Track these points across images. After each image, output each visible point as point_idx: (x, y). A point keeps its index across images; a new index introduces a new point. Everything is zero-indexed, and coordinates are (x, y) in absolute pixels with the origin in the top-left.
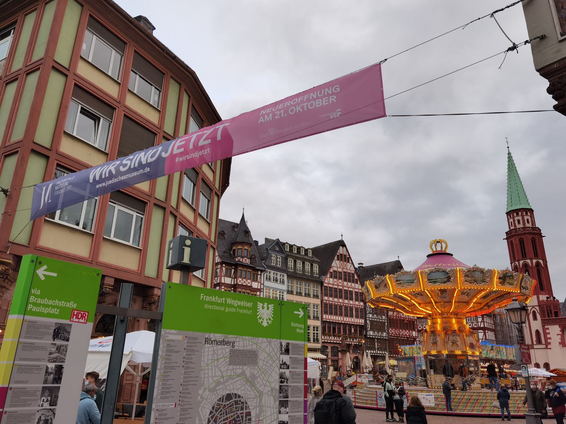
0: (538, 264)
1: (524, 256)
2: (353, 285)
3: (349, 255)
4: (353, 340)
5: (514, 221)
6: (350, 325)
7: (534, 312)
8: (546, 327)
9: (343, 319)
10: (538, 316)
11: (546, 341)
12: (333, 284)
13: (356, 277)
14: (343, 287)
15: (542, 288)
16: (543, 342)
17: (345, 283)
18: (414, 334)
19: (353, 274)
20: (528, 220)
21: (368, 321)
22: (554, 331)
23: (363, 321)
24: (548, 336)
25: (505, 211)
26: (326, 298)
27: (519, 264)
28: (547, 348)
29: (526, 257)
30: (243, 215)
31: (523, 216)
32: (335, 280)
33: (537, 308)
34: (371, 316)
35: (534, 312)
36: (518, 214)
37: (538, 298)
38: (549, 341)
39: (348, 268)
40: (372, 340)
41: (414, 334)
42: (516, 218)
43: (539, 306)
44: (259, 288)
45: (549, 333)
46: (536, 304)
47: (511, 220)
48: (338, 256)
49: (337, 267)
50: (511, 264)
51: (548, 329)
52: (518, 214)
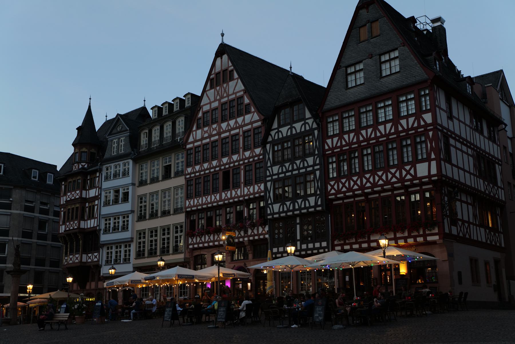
2: (240, 120)
4: (246, 232)
9: (221, 196)
12: (203, 138)
13: (247, 101)
17: (224, 125)
19: (242, 97)
21: (269, 184)
23: (262, 187)
26: (189, 170)
30: (90, 107)
32: (206, 129)
34: (276, 169)
39: (231, 92)
40: (288, 221)
44: (97, 194)
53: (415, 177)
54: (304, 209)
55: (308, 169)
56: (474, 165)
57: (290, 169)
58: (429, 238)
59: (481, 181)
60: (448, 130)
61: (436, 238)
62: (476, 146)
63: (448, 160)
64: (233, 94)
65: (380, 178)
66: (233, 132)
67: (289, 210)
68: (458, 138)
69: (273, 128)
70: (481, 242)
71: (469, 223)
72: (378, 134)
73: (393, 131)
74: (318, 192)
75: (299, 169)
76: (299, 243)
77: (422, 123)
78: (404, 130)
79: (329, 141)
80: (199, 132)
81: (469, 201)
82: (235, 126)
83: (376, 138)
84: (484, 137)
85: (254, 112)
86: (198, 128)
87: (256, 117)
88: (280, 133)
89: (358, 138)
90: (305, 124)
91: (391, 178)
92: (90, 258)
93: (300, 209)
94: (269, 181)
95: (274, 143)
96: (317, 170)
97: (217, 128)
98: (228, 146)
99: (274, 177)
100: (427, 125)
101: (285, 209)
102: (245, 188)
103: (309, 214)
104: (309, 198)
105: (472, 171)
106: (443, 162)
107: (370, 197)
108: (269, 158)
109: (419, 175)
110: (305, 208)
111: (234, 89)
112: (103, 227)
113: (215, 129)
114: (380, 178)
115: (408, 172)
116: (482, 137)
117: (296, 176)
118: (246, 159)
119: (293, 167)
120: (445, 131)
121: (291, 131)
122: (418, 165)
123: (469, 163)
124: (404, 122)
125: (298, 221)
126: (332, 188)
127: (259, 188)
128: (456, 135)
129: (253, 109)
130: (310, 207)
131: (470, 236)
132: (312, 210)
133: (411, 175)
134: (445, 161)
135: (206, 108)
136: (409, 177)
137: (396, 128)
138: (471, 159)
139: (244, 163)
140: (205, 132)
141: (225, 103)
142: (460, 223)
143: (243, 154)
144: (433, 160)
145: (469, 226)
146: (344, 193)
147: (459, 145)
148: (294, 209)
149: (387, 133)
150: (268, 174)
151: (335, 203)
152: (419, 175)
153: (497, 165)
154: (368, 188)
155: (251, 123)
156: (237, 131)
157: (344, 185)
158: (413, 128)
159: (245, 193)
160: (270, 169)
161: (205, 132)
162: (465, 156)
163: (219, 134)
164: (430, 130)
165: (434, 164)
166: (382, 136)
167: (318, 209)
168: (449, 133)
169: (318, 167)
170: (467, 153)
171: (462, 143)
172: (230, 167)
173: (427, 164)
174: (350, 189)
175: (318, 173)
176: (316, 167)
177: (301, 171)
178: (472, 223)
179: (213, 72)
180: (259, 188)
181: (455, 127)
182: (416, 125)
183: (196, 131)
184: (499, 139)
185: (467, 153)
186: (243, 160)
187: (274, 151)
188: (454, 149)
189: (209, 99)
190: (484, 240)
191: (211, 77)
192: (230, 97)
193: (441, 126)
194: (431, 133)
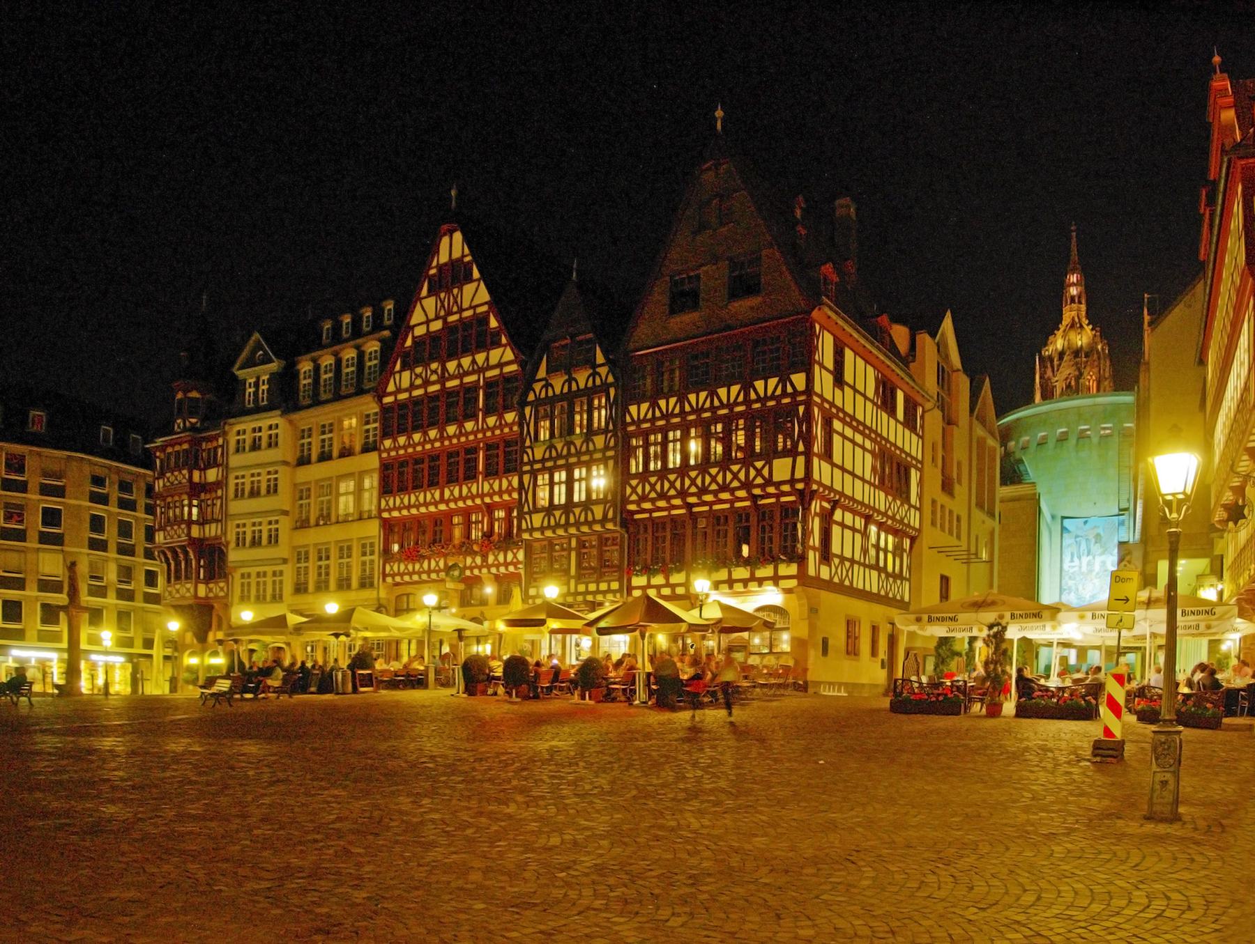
2: (480, 358)
12: (412, 387)
13: (493, 323)
21: (526, 478)
26: (388, 443)
32: (419, 370)
53: (769, 482)
56: (874, 469)
57: (565, 452)
59: (882, 495)
60: (832, 404)
62: (880, 436)
63: (828, 455)
65: (714, 479)
66: (467, 379)
68: (851, 420)
69: (538, 377)
70: (870, 593)
71: (852, 561)
72: (716, 403)
73: (741, 399)
75: (579, 453)
77: (789, 389)
78: (759, 399)
80: (406, 375)
81: (857, 526)
83: (713, 409)
84: (897, 421)
85: (505, 346)
86: (403, 369)
87: (509, 355)
89: (682, 408)
90: (594, 374)
91: (731, 481)
92: (211, 590)
95: (538, 402)
98: (456, 405)
100: (796, 392)
101: (552, 522)
104: (594, 508)
105: (867, 477)
106: (816, 461)
107: (696, 509)
109: (776, 478)
112: (231, 537)
113: (435, 372)
114: (714, 479)
116: (892, 421)
120: (827, 406)
121: (570, 387)
122: (776, 462)
123: (865, 464)
127: (510, 483)
128: (846, 414)
129: (504, 340)
131: (852, 583)
133: (763, 477)
134: (820, 457)
135: (420, 331)
136: (759, 481)
137: (747, 395)
138: (868, 457)
140: (417, 376)
142: (836, 561)
143: (484, 420)
144: (802, 453)
145: (852, 566)
147: (849, 432)
149: (732, 400)
150: (526, 459)
151: (637, 516)
152: (776, 478)
153: (913, 471)
155: (500, 365)
156: (473, 378)
158: (773, 397)
160: (529, 451)
161: (417, 376)
162: (859, 451)
163: (443, 380)
164: (801, 403)
165: (801, 460)
168: (834, 410)
170: (863, 447)
171: (855, 429)
173: (789, 460)
178: (859, 563)
180: (510, 483)
181: (844, 399)
182: (779, 392)
183: (400, 372)
184: (922, 427)
185: (863, 447)
186: (484, 431)
188: (840, 439)
190: (875, 590)
193: (821, 396)
194: (801, 409)
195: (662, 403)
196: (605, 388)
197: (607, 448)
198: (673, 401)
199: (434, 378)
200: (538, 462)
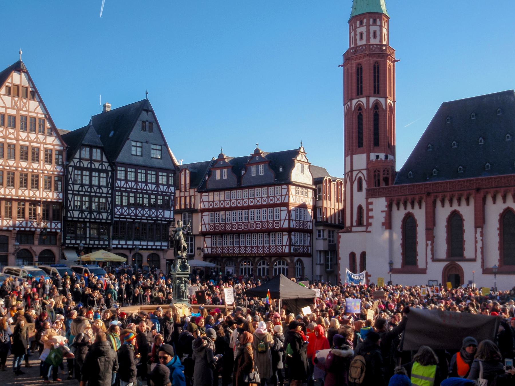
0: (377, 106)
1: (360, 93)
3: (34, 87)
5: (355, 35)
6: (35, 203)
7: (360, 180)
8: (370, 200)
9: (17, 192)
10: (364, 185)
11: (367, 221)
14: (17, 140)
15: (376, 143)
16: (365, 223)
17: (23, 135)
18: (167, 214)
20: (375, 33)
21: (70, 196)
22: (380, 204)
24: (370, 214)
25: (349, 17)
27: (351, 104)
28: (366, 231)
29: (362, 94)
31: (368, 25)
33: (365, 172)
34: (76, 187)
35: (360, 180)
36: (361, 23)
37: (368, 157)
38: (370, 221)
39: (32, 109)
41: (167, 214)
42: (359, 30)
43: (367, 169)
45: (371, 210)
46: (364, 165)
47: (352, 34)
48: (7, 87)
49: (6, 108)
50: (344, 105)
51: (371, 203)
52: (361, 23)
53: (163, 217)
54: (98, 219)
55: (103, 195)
57: (89, 190)
58: (163, 248)
61: (166, 248)
64: (34, 112)
66: (32, 144)
67: (86, 218)
69: (75, 157)
73: (156, 189)
74: (109, 211)
75: (95, 192)
76: (88, 240)
79: (119, 182)
82: (35, 140)
83: (146, 190)
87: (57, 142)
88: (81, 163)
89: (137, 187)
93: (95, 218)
94: (70, 194)
96: (109, 197)
97: (15, 134)
99: (75, 192)
100: (171, 193)
102: (44, 193)
103: (101, 222)
108: (71, 178)
109: (165, 217)
110: (99, 219)
111: (36, 109)
113: (13, 134)
115: (161, 214)
117: (93, 196)
118: (46, 170)
119: (91, 190)
121: (91, 166)
122: (165, 211)
124: (161, 187)
125: (88, 225)
126: (118, 211)
130: (103, 219)
132: (105, 221)
136: (160, 216)
139: (43, 173)
141: (22, 116)
143: (44, 166)
146: (125, 215)
148: (91, 218)
150: (70, 188)
152: (165, 217)
154: (139, 216)
156: (38, 145)
157: (125, 211)
158: (165, 192)
159: (44, 196)
160: (71, 185)
165: (172, 212)
166: (150, 190)
167: (108, 221)
169: (110, 196)
172: (27, 171)
174: (129, 214)
175: (109, 199)
176: (108, 195)
177: (97, 194)
179: (9, 80)
182: (167, 191)
186: (43, 170)
187: (74, 174)
189: (4, 103)
191: (7, 84)
192: (31, 114)
194: (172, 197)
195: (130, 183)
196: (106, 171)
197: (107, 193)
198: (144, 185)
199: (11, 136)
200: (76, 191)
